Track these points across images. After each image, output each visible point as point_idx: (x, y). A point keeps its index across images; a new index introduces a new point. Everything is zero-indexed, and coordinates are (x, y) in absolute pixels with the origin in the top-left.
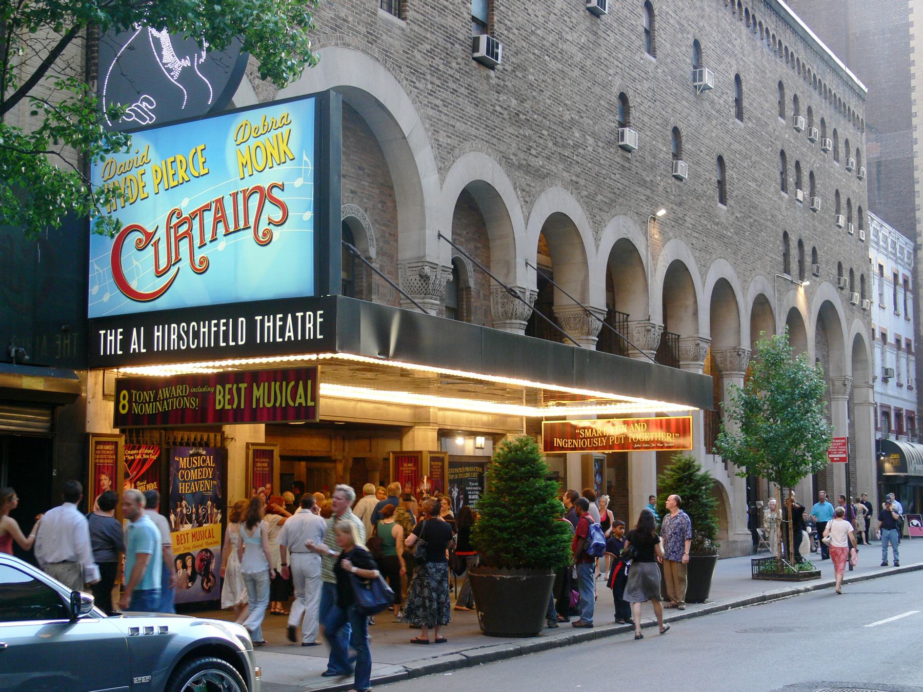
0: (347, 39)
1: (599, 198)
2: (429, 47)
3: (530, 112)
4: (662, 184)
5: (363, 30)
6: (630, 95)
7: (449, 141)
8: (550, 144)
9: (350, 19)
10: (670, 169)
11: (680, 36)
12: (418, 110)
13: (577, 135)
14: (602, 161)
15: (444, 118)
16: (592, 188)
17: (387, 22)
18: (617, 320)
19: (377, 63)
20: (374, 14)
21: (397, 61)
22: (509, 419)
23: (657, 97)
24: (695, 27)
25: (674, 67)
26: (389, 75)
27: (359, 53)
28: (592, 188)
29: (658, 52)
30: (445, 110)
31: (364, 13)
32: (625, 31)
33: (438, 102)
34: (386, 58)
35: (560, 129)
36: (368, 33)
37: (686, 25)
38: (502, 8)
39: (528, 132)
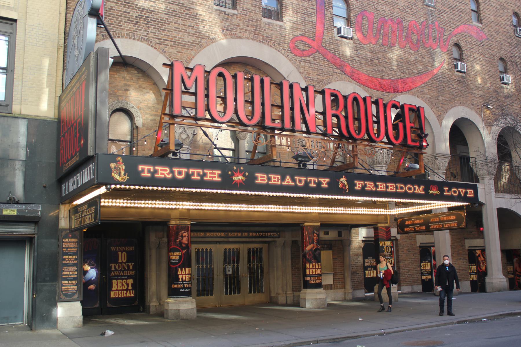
0: (239, 35)
1: (440, 98)
2: (301, 33)
3: (382, 58)
4: (492, 87)
5: (252, 29)
6: (462, 44)
7: (319, 77)
8: (399, 74)
9: (241, 24)
10: (499, 80)
11: (501, 12)
12: (294, 64)
13: (420, 67)
14: (441, 79)
15: (315, 66)
16: (435, 94)
17: (269, 24)
18: (471, 161)
19: (262, 44)
20: (259, 20)
21: (277, 41)
22: (380, 217)
23: (485, 43)
24: (513, 6)
25: (497, 27)
26: (272, 49)
27: (248, 41)
28: (435, 94)
29: (484, 21)
30: (315, 62)
31: (252, 21)
32: (457, 13)
33: (308, 59)
34: (268, 41)
35: (407, 65)
36: (254, 30)
37: (505, 5)
38: (357, 9)
39: (382, 68)
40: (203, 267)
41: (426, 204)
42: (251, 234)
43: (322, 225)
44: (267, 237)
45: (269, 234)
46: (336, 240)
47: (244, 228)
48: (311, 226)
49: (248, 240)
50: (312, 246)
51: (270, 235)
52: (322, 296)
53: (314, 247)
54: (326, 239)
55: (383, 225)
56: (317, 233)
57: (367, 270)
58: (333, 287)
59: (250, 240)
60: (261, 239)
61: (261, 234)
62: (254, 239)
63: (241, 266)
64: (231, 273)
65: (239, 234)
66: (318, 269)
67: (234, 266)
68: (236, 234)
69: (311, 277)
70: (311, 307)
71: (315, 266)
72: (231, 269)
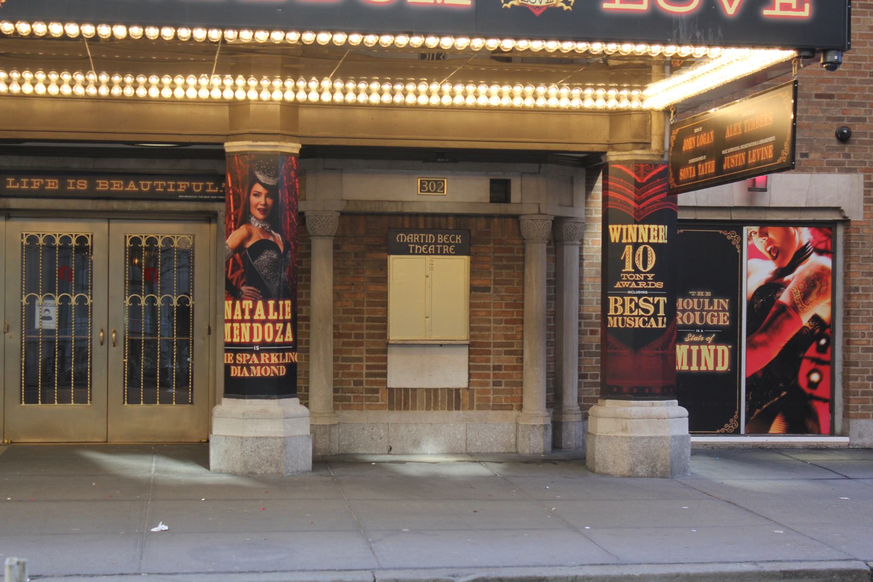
40: (168, 301)
41: (688, 62)
42: (102, 185)
43: (308, 152)
44: (174, 198)
45: (183, 185)
46: (489, 217)
47: (75, 164)
48: (243, 154)
49: (89, 205)
50: (242, 232)
51: (189, 191)
52: (272, 429)
53: (249, 236)
54: (429, 209)
55: (626, 156)
56: (271, 182)
57: (681, 341)
58: (465, 399)
59: (102, 205)
60: (146, 205)
61: (146, 186)
62: (115, 205)
63: (97, 300)
64: (52, 325)
65: (52, 184)
66: (263, 322)
67: (65, 300)
68: (36, 183)
69: (235, 352)
70: (223, 467)
71: (252, 312)
72: (54, 313)
